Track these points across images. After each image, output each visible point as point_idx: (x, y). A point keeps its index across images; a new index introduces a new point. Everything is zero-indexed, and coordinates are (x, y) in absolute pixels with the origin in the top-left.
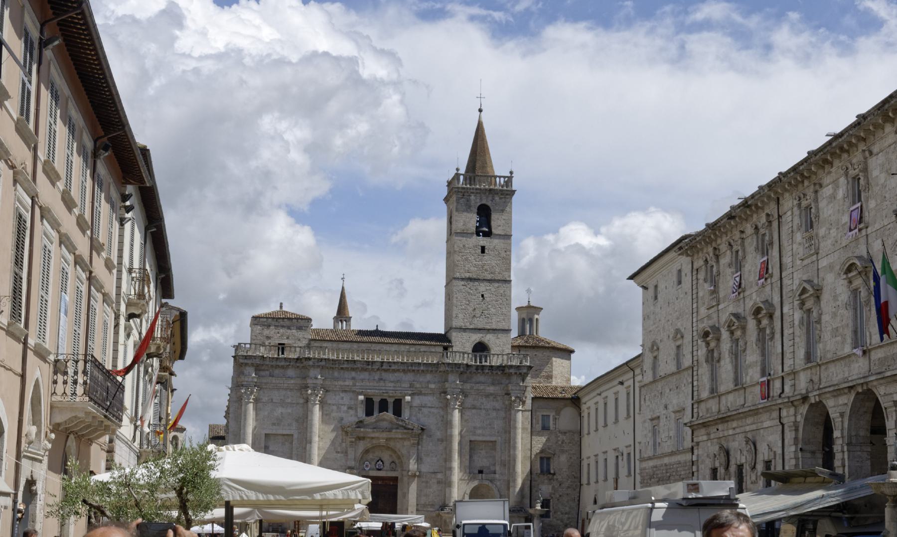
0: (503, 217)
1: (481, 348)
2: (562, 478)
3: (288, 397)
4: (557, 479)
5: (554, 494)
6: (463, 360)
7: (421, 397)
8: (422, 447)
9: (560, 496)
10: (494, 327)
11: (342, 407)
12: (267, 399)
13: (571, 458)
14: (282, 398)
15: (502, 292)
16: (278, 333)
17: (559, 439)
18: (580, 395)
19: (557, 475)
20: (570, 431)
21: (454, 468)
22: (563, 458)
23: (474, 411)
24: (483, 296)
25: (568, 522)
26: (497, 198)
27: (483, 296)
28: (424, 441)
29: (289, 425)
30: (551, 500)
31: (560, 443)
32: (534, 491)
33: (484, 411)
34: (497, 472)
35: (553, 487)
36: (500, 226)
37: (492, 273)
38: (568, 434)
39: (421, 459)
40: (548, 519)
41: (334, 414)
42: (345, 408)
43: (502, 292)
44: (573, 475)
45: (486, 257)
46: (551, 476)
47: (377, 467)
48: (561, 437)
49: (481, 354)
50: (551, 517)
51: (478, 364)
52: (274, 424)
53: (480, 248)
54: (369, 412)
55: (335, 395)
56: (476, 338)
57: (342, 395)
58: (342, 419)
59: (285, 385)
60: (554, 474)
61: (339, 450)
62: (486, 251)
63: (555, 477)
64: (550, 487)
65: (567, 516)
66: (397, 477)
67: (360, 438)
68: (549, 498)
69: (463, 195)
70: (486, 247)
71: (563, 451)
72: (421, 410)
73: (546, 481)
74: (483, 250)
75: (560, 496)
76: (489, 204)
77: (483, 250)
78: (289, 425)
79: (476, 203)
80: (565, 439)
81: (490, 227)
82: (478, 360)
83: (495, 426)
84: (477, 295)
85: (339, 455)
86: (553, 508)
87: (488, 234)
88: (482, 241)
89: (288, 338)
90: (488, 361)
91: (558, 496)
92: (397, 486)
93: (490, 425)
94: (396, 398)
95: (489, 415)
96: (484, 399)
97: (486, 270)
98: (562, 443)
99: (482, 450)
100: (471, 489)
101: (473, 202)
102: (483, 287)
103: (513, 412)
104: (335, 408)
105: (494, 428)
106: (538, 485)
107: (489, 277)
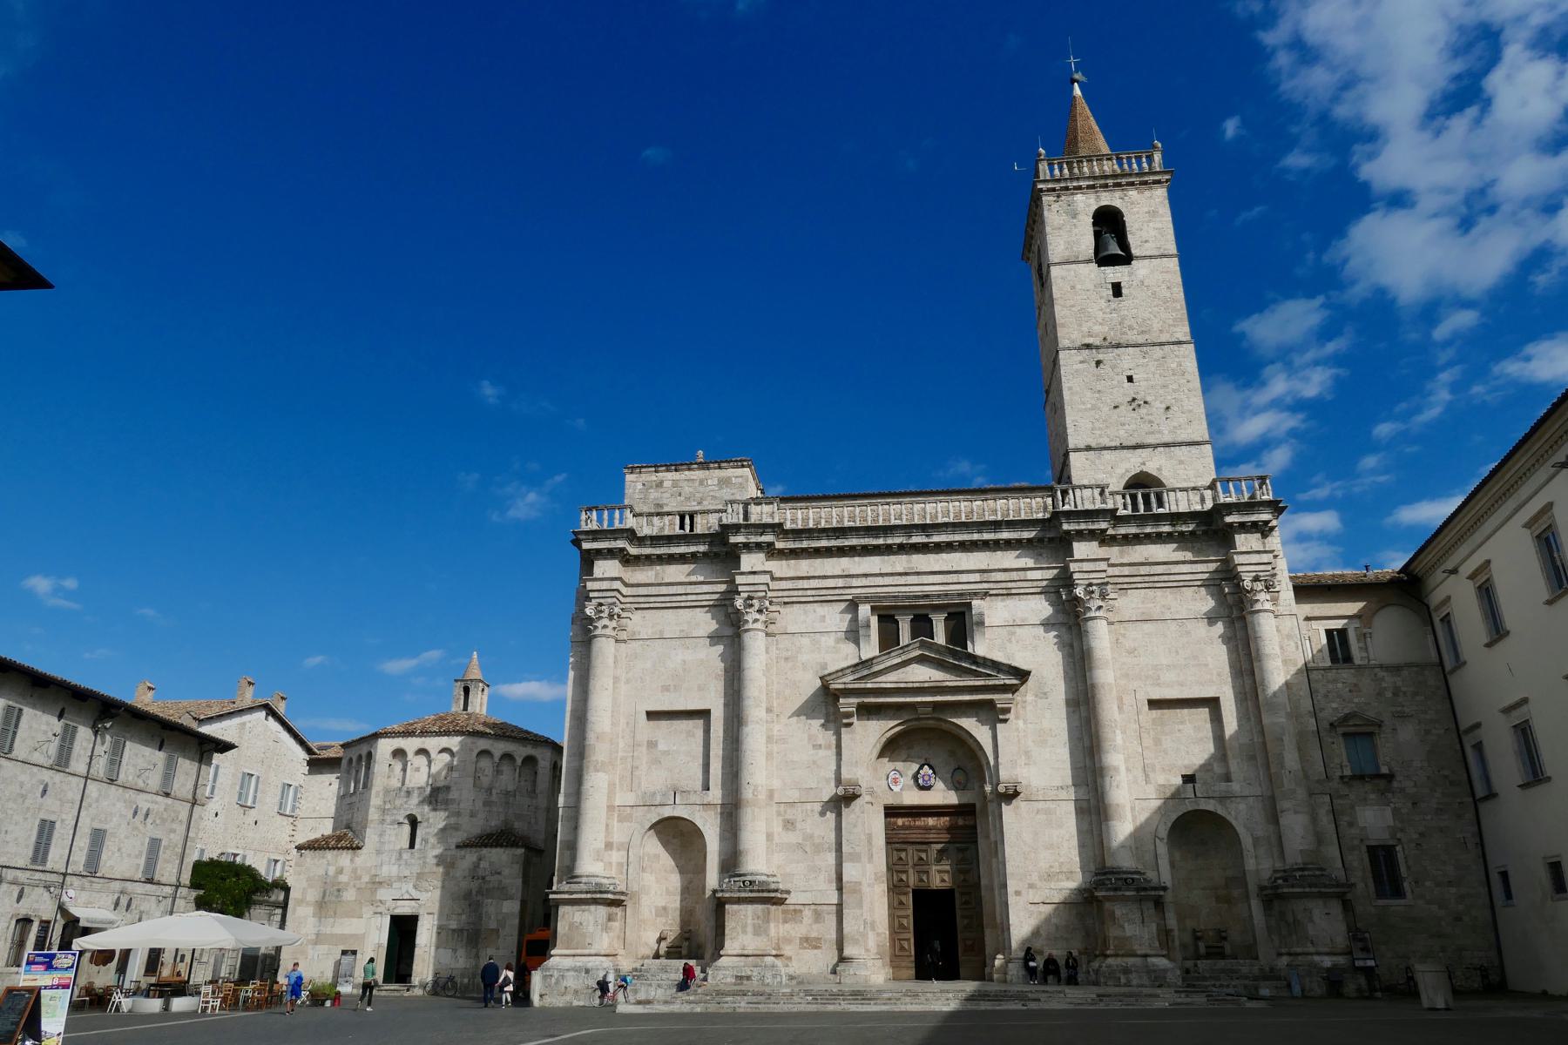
0: (1151, 224)
1: (1142, 484)
2: (1415, 785)
3: (698, 624)
4: (1402, 790)
5: (1402, 830)
6: (1104, 502)
7: (1011, 603)
8: (1025, 722)
9: (1422, 835)
10: (1167, 438)
11: (823, 639)
12: (650, 631)
13: (1428, 732)
14: (685, 627)
15: (1174, 366)
16: (680, 495)
17: (1384, 685)
18: (1418, 568)
19: (1399, 778)
20: (1409, 665)
21: (1116, 769)
22: (1407, 733)
23: (1147, 627)
24: (1130, 379)
25: (1461, 907)
26: (1133, 193)
27: (1130, 379)
28: (1029, 708)
29: (700, 688)
30: (1398, 848)
31: (1389, 694)
32: (1343, 822)
33: (1173, 626)
34: (1234, 777)
35: (1396, 812)
36: (1146, 241)
37: (1143, 332)
38: (1405, 673)
39: (1027, 753)
40: (1402, 902)
41: (804, 658)
42: (829, 641)
43: (1174, 366)
44: (1446, 777)
45: (1125, 303)
46: (1382, 783)
47: (920, 781)
48: (1389, 680)
49: (1147, 490)
50: (1409, 894)
51: (1142, 512)
52: (666, 689)
53: (1110, 286)
54: (889, 640)
55: (805, 612)
56: (1132, 464)
57: (821, 610)
58: (824, 666)
59: (690, 598)
60: (1390, 777)
61: (821, 741)
62: (1124, 291)
63: (1395, 784)
64: (1388, 812)
65: (1453, 890)
66: (974, 805)
67: (867, 711)
68: (1391, 843)
69: (1058, 196)
70: (1122, 285)
71: (1402, 716)
72: (1014, 633)
73: (1372, 796)
74: (1117, 290)
75: (1422, 835)
76: (1117, 203)
77: (1117, 290)
78: (700, 688)
79: (1089, 206)
80: (1399, 684)
81: (1124, 244)
82: (1141, 507)
83: (1209, 659)
84: (1120, 377)
85: (822, 753)
86: (1409, 868)
87: (1126, 259)
88: (1115, 273)
89: (699, 503)
90: (1167, 505)
91: (1415, 836)
92: (975, 827)
93: (1196, 658)
94: (952, 610)
95: (1188, 633)
96: (1170, 597)
97: (1131, 328)
98: (1395, 694)
99: (1182, 723)
100: (1169, 825)
101: (1081, 205)
102: (1128, 360)
103: (1249, 618)
104: (805, 641)
105: (1206, 665)
106: (1352, 807)
107: (1141, 339)
